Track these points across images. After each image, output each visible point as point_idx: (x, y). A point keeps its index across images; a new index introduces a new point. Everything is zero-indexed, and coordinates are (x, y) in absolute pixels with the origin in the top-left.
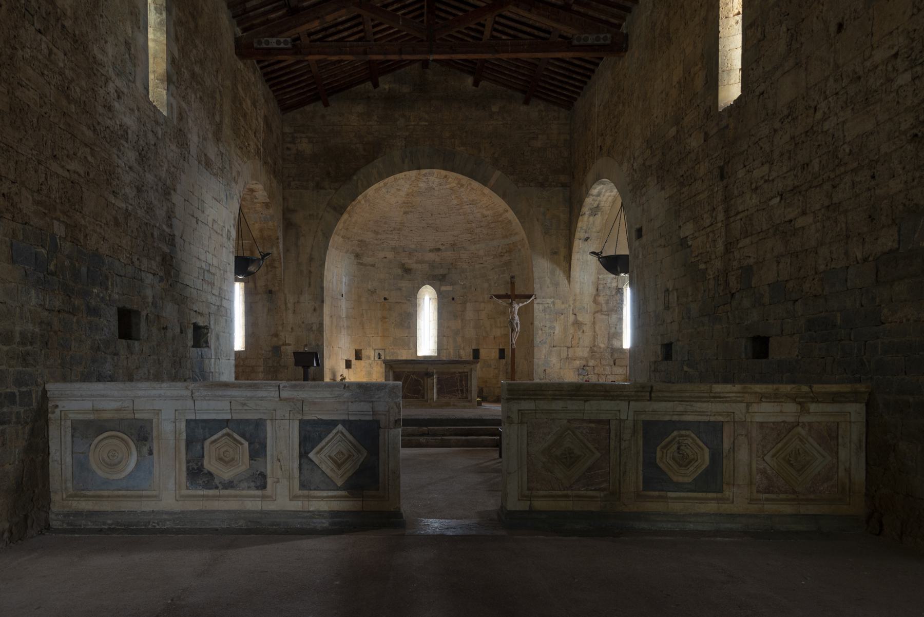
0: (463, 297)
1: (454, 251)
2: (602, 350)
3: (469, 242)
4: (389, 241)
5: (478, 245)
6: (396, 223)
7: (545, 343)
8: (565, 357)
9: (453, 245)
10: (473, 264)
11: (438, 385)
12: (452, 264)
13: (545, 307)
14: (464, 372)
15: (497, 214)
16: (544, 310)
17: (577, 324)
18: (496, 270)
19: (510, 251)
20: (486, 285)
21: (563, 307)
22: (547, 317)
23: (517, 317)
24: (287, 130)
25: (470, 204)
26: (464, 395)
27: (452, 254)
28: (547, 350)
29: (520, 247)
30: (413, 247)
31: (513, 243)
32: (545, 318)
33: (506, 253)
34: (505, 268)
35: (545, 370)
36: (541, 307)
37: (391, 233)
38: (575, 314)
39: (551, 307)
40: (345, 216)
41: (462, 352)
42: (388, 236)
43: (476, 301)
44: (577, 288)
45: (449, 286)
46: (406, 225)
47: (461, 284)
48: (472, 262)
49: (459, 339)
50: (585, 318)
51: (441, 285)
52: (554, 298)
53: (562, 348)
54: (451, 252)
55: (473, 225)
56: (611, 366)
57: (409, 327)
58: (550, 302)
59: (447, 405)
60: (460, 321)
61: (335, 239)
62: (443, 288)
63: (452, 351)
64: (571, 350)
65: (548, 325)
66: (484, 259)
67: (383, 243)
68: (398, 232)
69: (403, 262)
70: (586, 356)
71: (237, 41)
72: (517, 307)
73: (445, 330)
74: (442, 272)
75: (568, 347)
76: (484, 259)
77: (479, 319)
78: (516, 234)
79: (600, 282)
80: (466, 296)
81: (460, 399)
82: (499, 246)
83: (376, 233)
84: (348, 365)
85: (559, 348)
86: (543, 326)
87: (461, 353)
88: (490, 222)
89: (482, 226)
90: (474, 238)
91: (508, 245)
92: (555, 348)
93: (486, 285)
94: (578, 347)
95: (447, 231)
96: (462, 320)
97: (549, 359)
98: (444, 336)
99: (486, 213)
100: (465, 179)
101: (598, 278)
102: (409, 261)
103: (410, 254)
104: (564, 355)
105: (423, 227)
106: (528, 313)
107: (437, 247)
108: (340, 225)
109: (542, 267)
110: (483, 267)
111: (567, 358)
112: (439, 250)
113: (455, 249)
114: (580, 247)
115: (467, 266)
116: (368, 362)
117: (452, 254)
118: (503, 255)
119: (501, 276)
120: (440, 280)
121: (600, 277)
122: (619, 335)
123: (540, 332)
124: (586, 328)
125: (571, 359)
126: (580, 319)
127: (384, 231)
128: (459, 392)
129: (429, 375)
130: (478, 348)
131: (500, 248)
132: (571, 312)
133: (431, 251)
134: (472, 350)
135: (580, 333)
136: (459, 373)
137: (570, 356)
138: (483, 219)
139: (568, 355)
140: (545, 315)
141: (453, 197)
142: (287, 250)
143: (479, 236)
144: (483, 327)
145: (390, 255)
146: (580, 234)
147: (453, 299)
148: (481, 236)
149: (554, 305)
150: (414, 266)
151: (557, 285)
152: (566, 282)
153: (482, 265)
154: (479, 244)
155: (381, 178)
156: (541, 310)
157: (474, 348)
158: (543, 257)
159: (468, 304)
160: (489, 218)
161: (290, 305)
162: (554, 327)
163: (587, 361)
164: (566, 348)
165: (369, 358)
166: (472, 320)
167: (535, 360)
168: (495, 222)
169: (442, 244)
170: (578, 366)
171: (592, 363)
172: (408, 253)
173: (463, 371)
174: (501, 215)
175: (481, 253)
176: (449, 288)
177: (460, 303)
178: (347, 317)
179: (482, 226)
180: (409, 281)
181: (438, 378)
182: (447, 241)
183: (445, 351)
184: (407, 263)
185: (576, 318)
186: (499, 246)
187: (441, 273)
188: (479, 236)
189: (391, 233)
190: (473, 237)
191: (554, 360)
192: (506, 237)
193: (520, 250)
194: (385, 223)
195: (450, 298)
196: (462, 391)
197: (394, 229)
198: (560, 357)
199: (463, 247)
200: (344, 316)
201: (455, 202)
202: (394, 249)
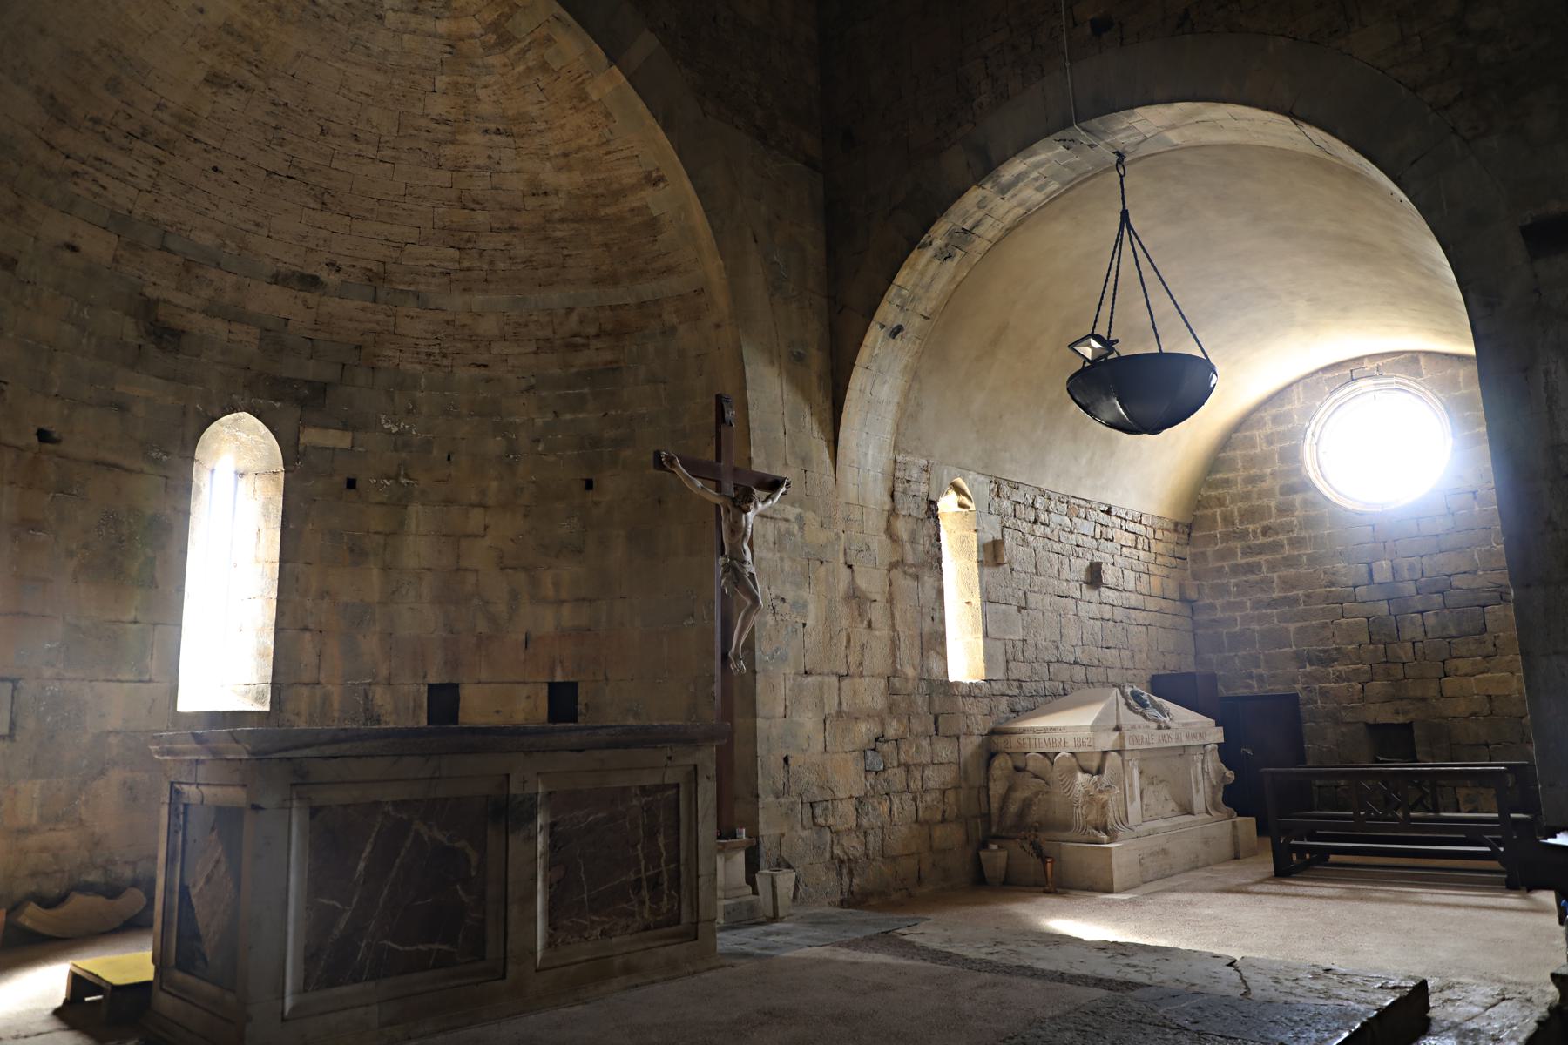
0: (396, 478)
1: (375, 301)
2: (910, 685)
3: (446, 279)
4: (104, 181)
5: (480, 297)
6: (159, 107)
7: (784, 659)
8: (833, 712)
9: (376, 280)
10: (445, 362)
11: (550, 867)
12: (359, 347)
13: (779, 531)
14: (662, 788)
15: (600, 190)
17: (855, 597)
18: (544, 394)
19: (618, 333)
20: (495, 445)
21: (822, 537)
22: (787, 565)
25: (498, 132)
26: (665, 904)
27: (363, 309)
28: (789, 683)
29: (670, 318)
30: (207, 240)
31: (641, 305)
32: (782, 571)
33: (598, 336)
34: (586, 390)
35: (786, 760)
36: (770, 530)
37: (124, 142)
38: (850, 567)
39: (793, 535)
41: (380, 696)
42: (107, 154)
43: (448, 502)
45: (338, 433)
46: (198, 135)
47: (389, 432)
48: (444, 356)
49: (370, 644)
50: (871, 581)
51: (303, 423)
52: (801, 506)
53: (827, 679)
54: (359, 304)
55: (481, 217)
56: (930, 736)
58: (792, 518)
60: (375, 571)
62: (311, 436)
63: (335, 691)
64: (846, 683)
65: (789, 596)
66: (497, 348)
67: (76, 173)
68: (159, 153)
69: (150, 292)
70: (879, 707)
73: (309, 604)
74: (311, 370)
75: (840, 677)
76: (494, 351)
77: (458, 570)
78: (669, 270)
79: (898, 474)
80: (407, 476)
81: (647, 928)
82: (570, 310)
83: (59, 113)
85: (819, 678)
86: (777, 597)
87: (379, 700)
88: (557, 216)
89: (512, 228)
90: (469, 269)
91: (611, 308)
92: (810, 679)
93: (495, 445)
94: (861, 675)
95: (362, 219)
96: (386, 569)
97: (796, 719)
98: (306, 629)
99: (549, 176)
101: (895, 461)
102: (180, 298)
103: (188, 265)
104: (831, 707)
105: (270, 173)
107: (310, 271)
110: (488, 380)
111: (840, 714)
112: (311, 282)
113: (381, 294)
114: (876, 351)
115: (419, 367)
117: (363, 309)
118: (587, 346)
119: (568, 416)
120: (303, 403)
121: (900, 458)
122: (935, 641)
123: (770, 619)
124: (877, 613)
125: (849, 715)
126: (862, 583)
127: (96, 121)
128: (645, 893)
130: (455, 681)
131: (574, 318)
132: (842, 561)
133: (277, 279)
134: (424, 689)
135: (862, 628)
136: (643, 789)
137: (845, 707)
138: (531, 202)
139: (840, 703)
140: (782, 559)
141: (442, 81)
143: (492, 263)
144: (476, 601)
147: (351, 484)
148: (500, 265)
149: (802, 527)
150: (198, 323)
152: (826, 456)
153: (483, 371)
154: (486, 291)
156: (771, 540)
157: (433, 680)
158: (772, 363)
159: (414, 509)
160: (557, 203)
162: (805, 606)
163: (883, 723)
164: (834, 679)
166: (429, 569)
167: (760, 722)
168: (580, 221)
169: (331, 264)
170: (866, 740)
171: (893, 729)
172: (178, 259)
173: (657, 781)
174: (619, 194)
175: (488, 326)
176: (337, 439)
177: (382, 504)
179: (512, 228)
180: (167, 379)
181: (553, 825)
182: (357, 259)
183: (305, 691)
184: (166, 302)
185: (853, 579)
186: (570, 310)
187: (310, 378)
188: (492, 263)
189: (124, 142)
190: (466, 264)
191: (808, 722)
193: (668, 332)
194: (113, 85)
195: (340, 480)
196: (655, 883)
197: (144, 134)
198: (823, 710)
199: (417, 295)
201: (439, 106)
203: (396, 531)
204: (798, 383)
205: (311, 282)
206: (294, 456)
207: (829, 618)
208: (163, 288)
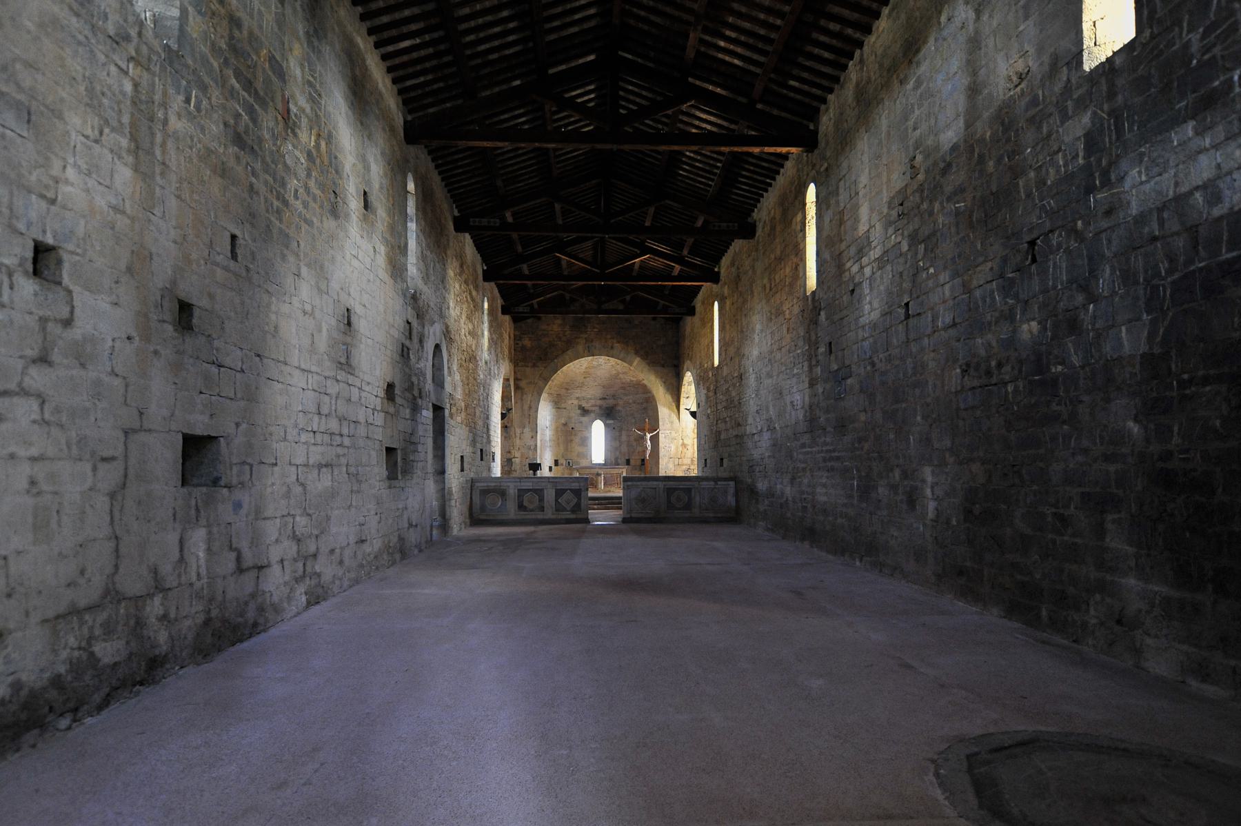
9: (614, 396)
16: (665, 437)
17: (684, 445)
20: (633, 421)
23: (649, 442)
24: (517, 333)
40: (550, 382)
44: (683, 423)
57: (587, 446)
59: (609, 491)
61: (544, 395)
71: (502, 306)
72: (648, 436)
83: (567, 389)
84: (550, 468)
93: (633, 421)
100: (619, 362)
106: (655, 440)
108: (547, 387)
109: (664, 412)
112: (605, 399)
116: (562, 467)
124: (689, 447)
126: (685, 442)
129: (598, 475)
142: (516, 403)
145: (576, 402)
146: (683, 395)
151: (672, 422)
155: (571, 361)
159: (623, 432)
161: (518, 435)
165: (562, 465)
175: (631, 401)
176: (611, 422)
178: (550, 440)
191: (671, 466)
192: (644, 393)
200: (548, 439)
202: (578, 398)
203: (620, 436)
204: (669, 408)
205: (605, 399)
206: (606, 425)
207: (677, 448)
208: (584, 405)
